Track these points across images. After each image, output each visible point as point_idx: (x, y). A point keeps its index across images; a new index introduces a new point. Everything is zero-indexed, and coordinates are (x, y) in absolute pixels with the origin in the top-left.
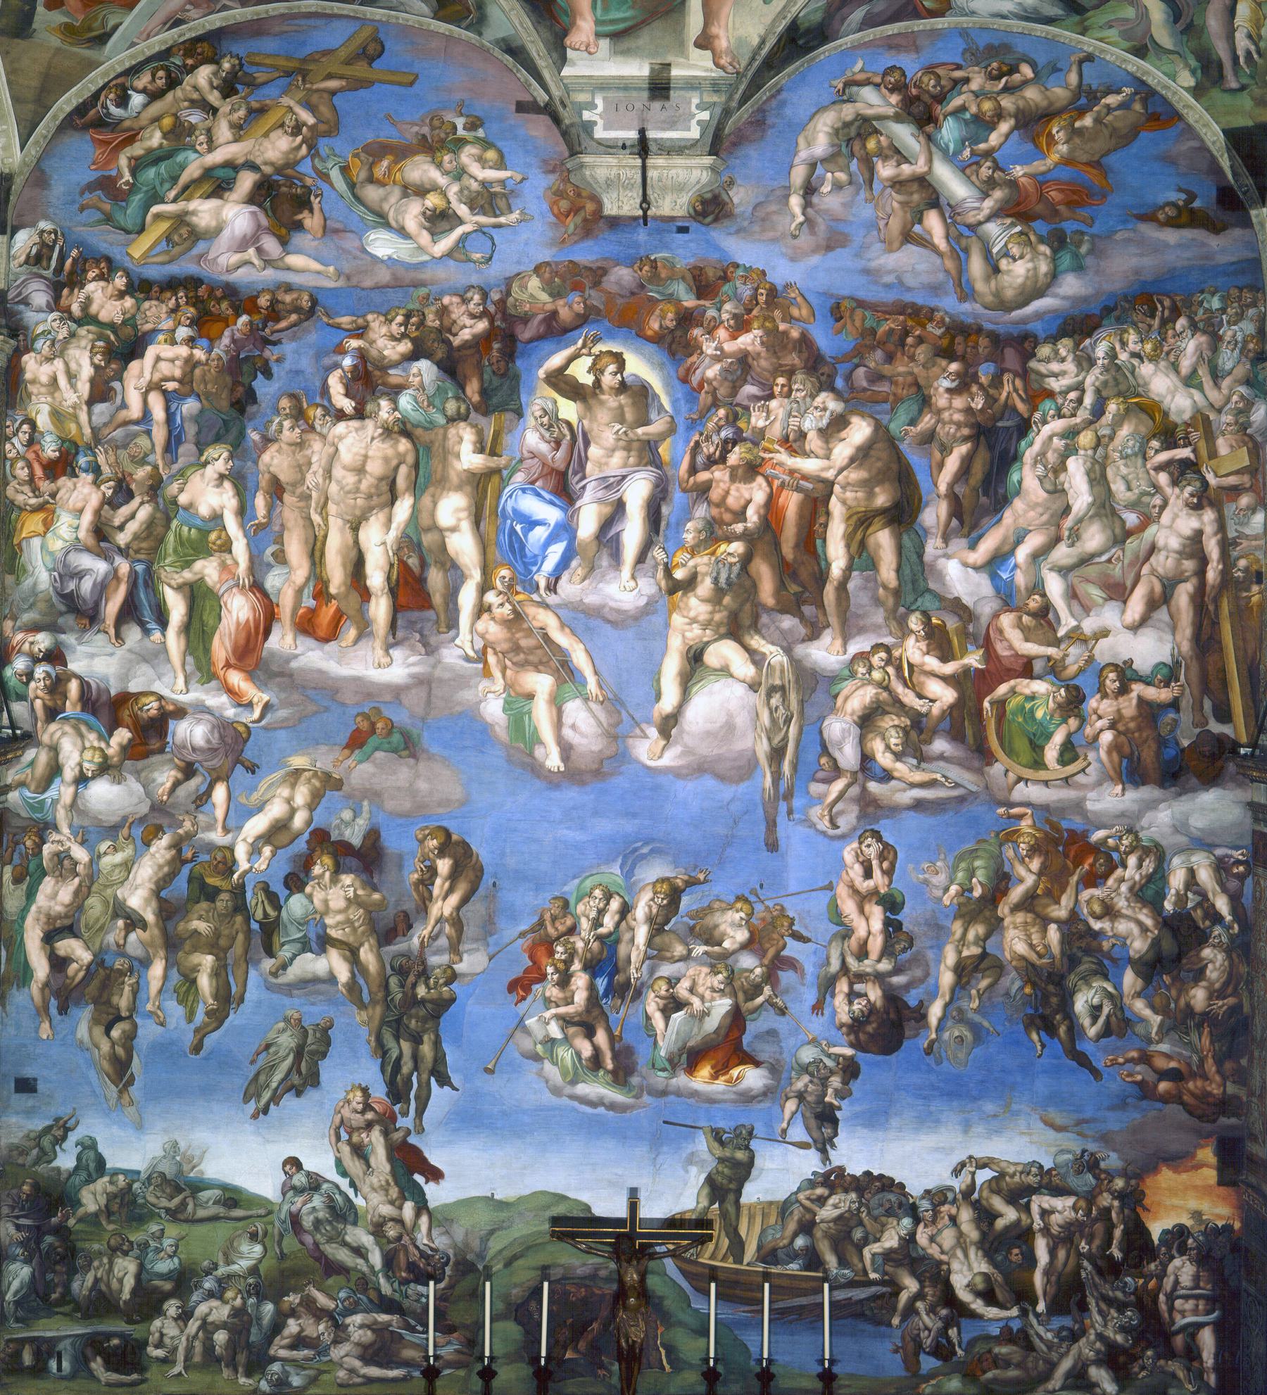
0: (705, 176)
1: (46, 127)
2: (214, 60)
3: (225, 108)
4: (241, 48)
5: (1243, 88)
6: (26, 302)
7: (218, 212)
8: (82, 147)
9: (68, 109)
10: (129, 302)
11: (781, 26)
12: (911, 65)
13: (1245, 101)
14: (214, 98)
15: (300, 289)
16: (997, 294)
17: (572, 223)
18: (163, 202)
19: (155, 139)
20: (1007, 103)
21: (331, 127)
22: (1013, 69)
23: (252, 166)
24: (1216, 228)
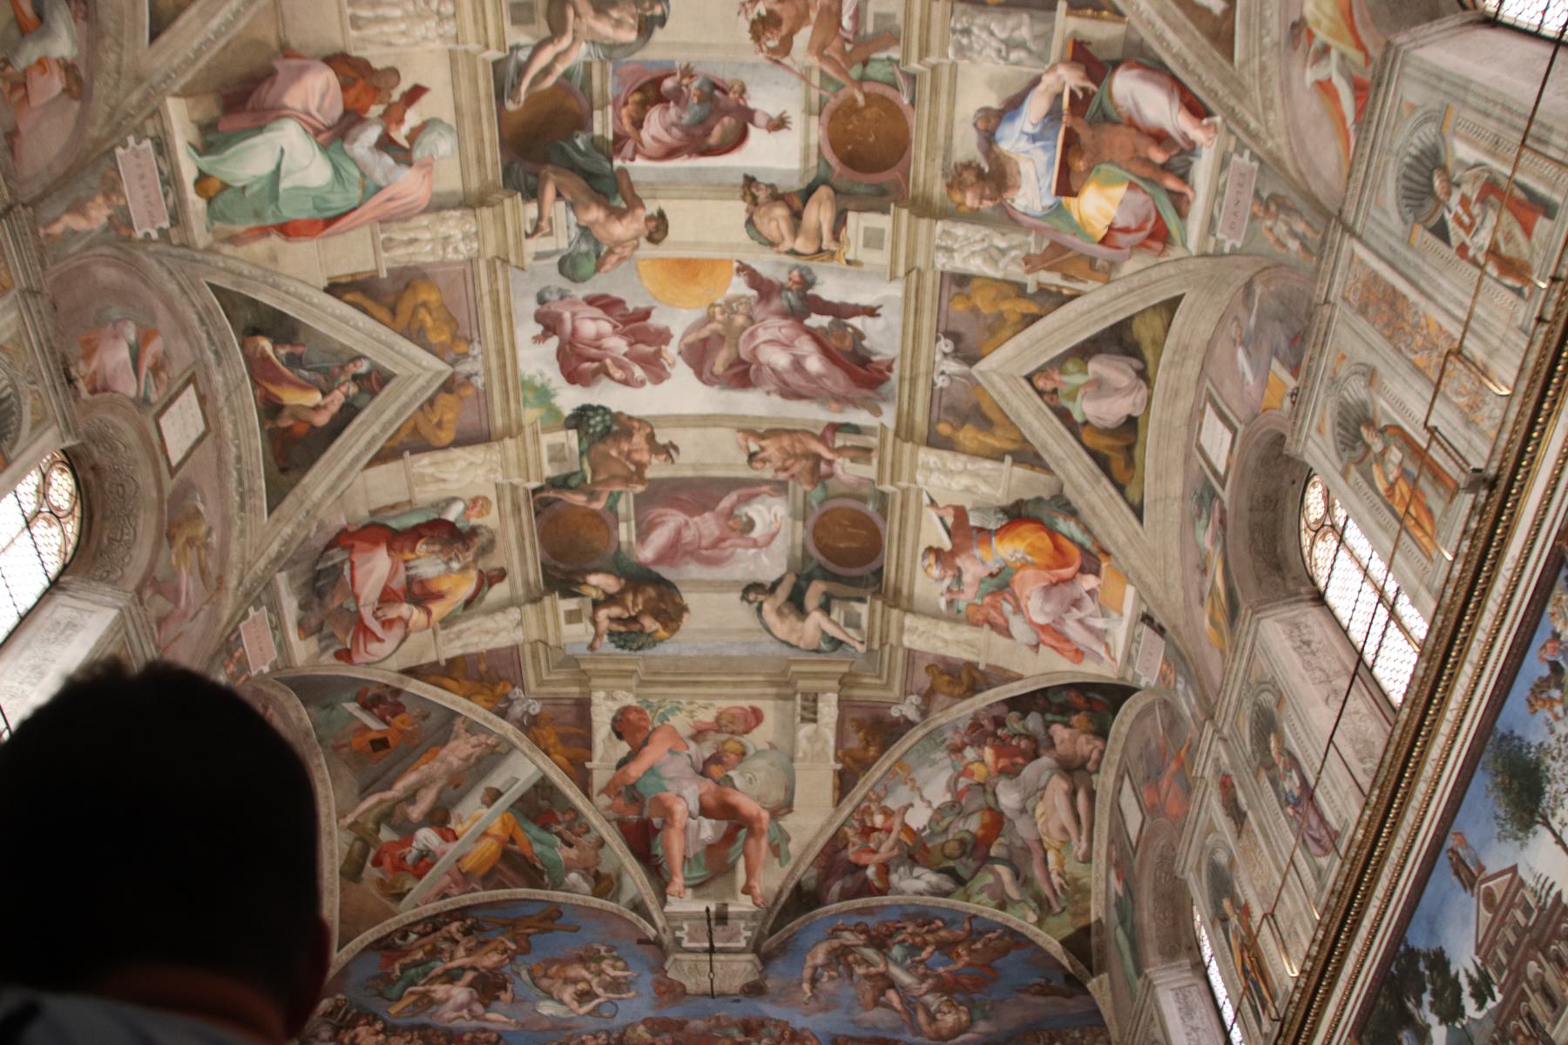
0: (749, 967)
1: (356, 944)
2: (463, 920)
3: (464, 941)
4: (479, 914)
5: (1064, 909)
6: (316, 1036)
7: (448, 991)
8: (376, 958)
9: (371, 939)
10: (381, 1037)
11: (791, 885)
12: (871, 922)
13: (1066, 917)
14: (458, 936)
15: (491, 1031)
16: (938, 1032)
17: (666, 998)
18: (416, 985)
19: (419, 955)
20: (929, 938)
21: (526, 950)
22: (930, 923)
23: (474, 968)
24: (1069, 996)
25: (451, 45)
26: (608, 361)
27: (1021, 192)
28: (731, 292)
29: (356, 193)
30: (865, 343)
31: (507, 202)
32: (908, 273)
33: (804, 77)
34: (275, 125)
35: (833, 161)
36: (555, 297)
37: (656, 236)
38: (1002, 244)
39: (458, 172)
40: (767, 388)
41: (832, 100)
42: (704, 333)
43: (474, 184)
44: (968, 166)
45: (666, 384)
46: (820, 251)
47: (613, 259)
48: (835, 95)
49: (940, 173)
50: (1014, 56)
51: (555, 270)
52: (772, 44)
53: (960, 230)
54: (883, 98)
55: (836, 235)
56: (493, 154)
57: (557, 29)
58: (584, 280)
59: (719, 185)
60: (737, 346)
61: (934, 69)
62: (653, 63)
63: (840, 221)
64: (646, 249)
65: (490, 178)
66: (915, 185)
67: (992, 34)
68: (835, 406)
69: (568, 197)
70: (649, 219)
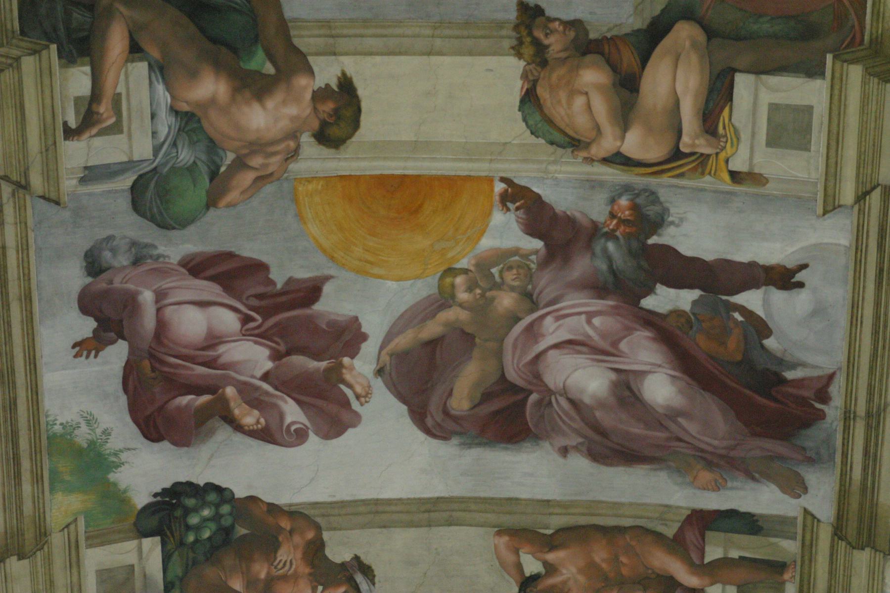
26: (230, 391)
28: (487, 243)
30: (770, 343)
31: (29, 63)
32: (861, 197)
36: (123, 260)
37: (334, 132)
40: (563, 442)
42: (432, 329)
45: (350, 432)
46: (677, 155)
47: (248, 177)
51: (124, 203)
58: (183, 223)
59: (467, 24)
60: (499, 354)
68: (706, 476)
69: (155, 53)
70: (321, 95)
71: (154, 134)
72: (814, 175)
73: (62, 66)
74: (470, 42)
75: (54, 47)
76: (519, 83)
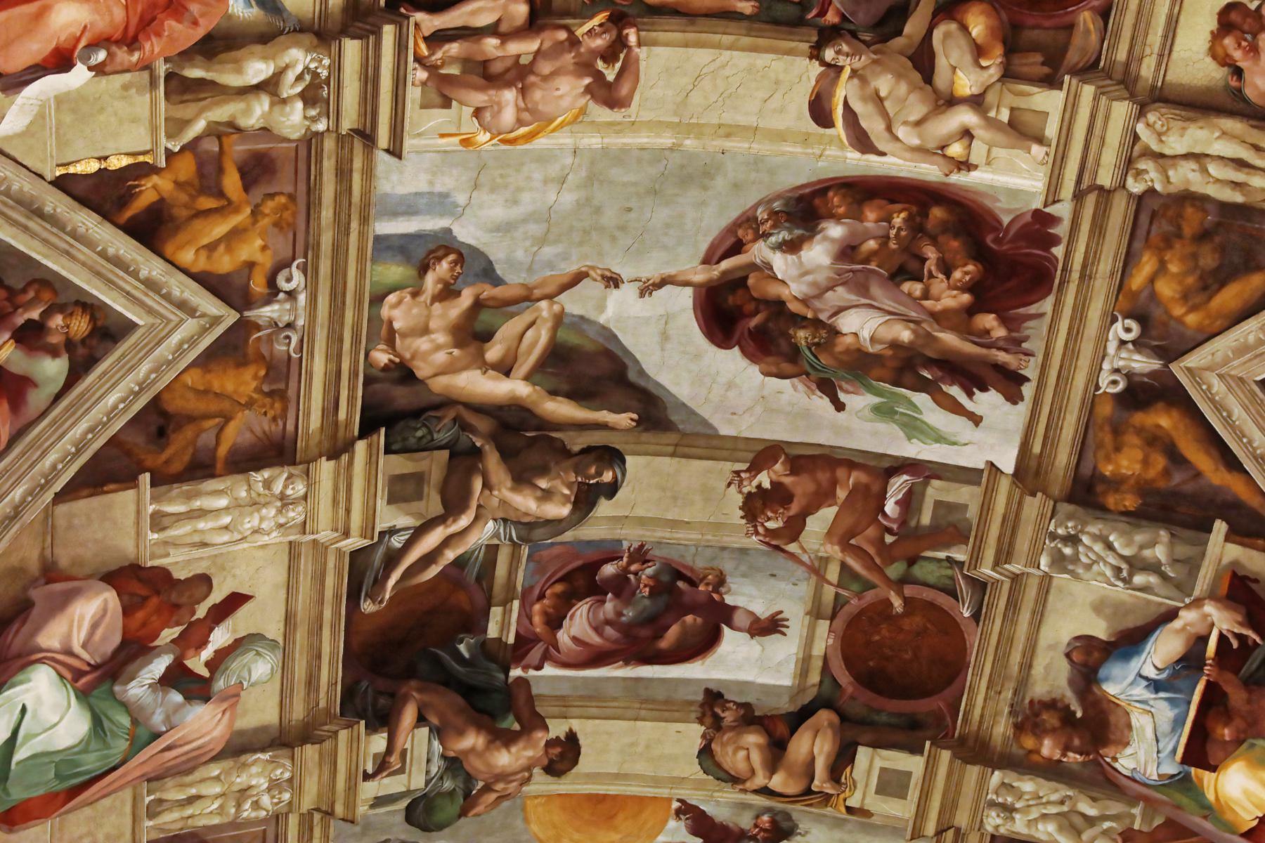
25: (292, 538)
27: (1129, 751)
29: (122, 745)
31: (343, 735)
32: (939, 833)
33: (817, 570)
34: (20, 677)
35: (844, 678)
37: (559, 766)
38: (1092, 812)
39: (276, 699)
41: (854, 602)
43: (298, 712)
44: (1051, 705)
46: (808, 791)
47: (493, 796)
48: (859, 595)
49: (1006, 710)
50: (1139, 579)
51: (400, 818)
52: (771, 525)
53: (1028, 785)
54: (931, 605)
55: (835, 772)
56: (331, 673)
57: (454, 503)
58: (440, 827)
59: (666, 702)
61: (1016, 578)
62: (589, 542)
63: (842, 759)
64: (541, 784)
65: (322, 704)
66: (965, 720)
67: (1110, 547)
69: (435, 720)
70: (550, 744)
71: (428, 772)
72: (907, 816)
73: (367, 734)
74: (666, 714)
75: (363, 722)
76: (699, 741)
